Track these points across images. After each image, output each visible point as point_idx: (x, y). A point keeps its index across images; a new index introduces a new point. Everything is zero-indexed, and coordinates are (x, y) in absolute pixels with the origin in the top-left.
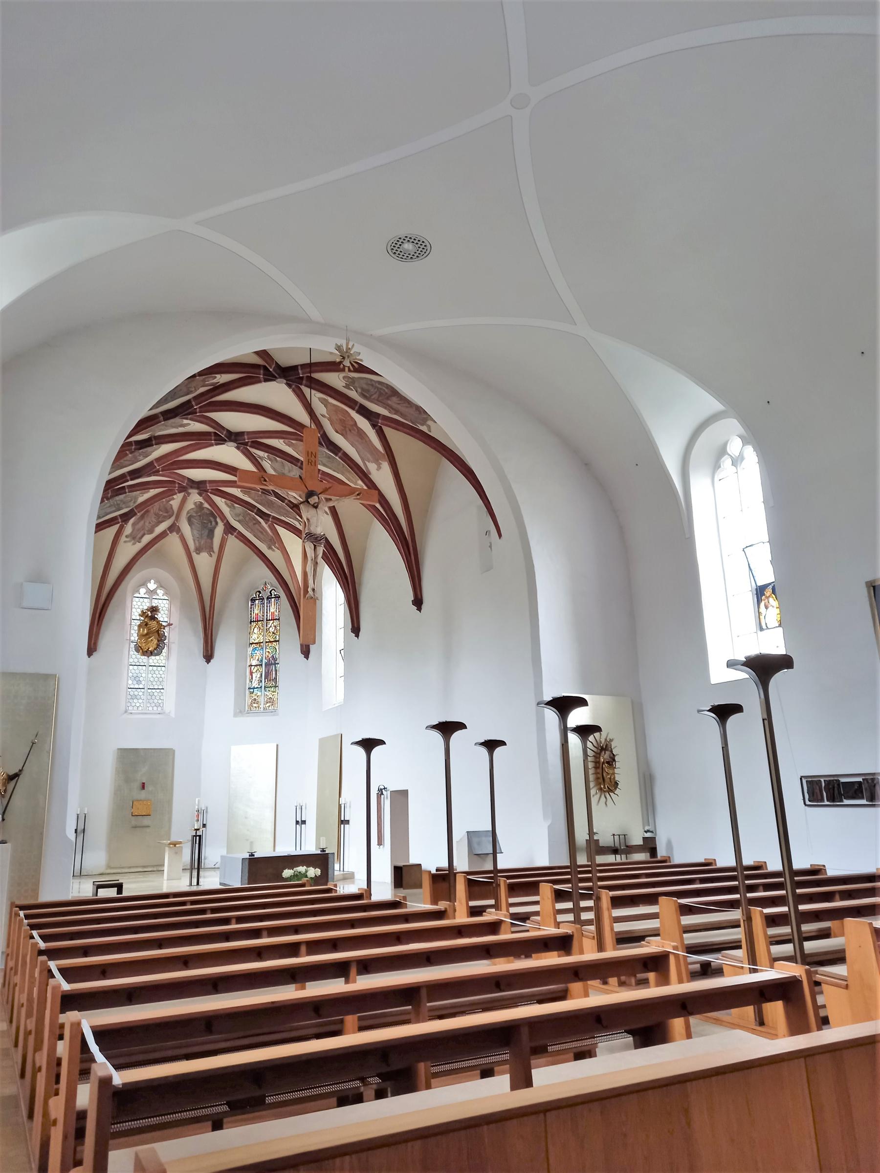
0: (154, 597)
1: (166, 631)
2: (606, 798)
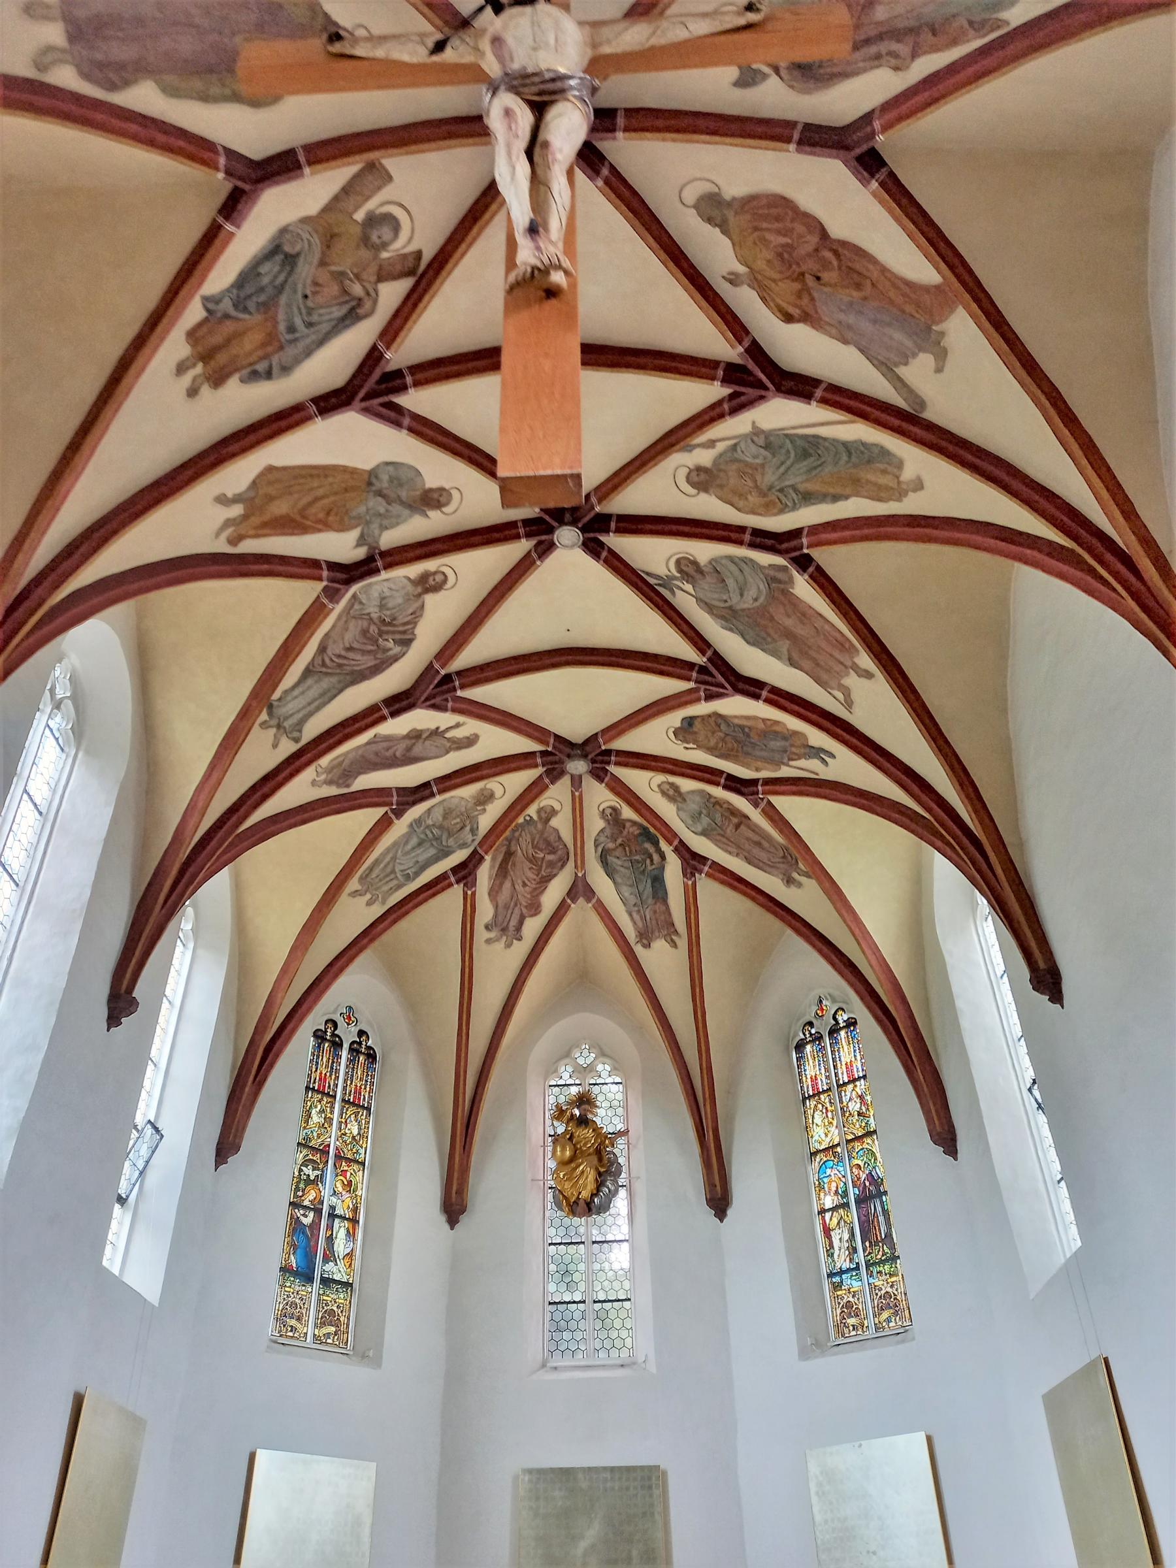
0: (592, 1081)
1: (620, 1149)
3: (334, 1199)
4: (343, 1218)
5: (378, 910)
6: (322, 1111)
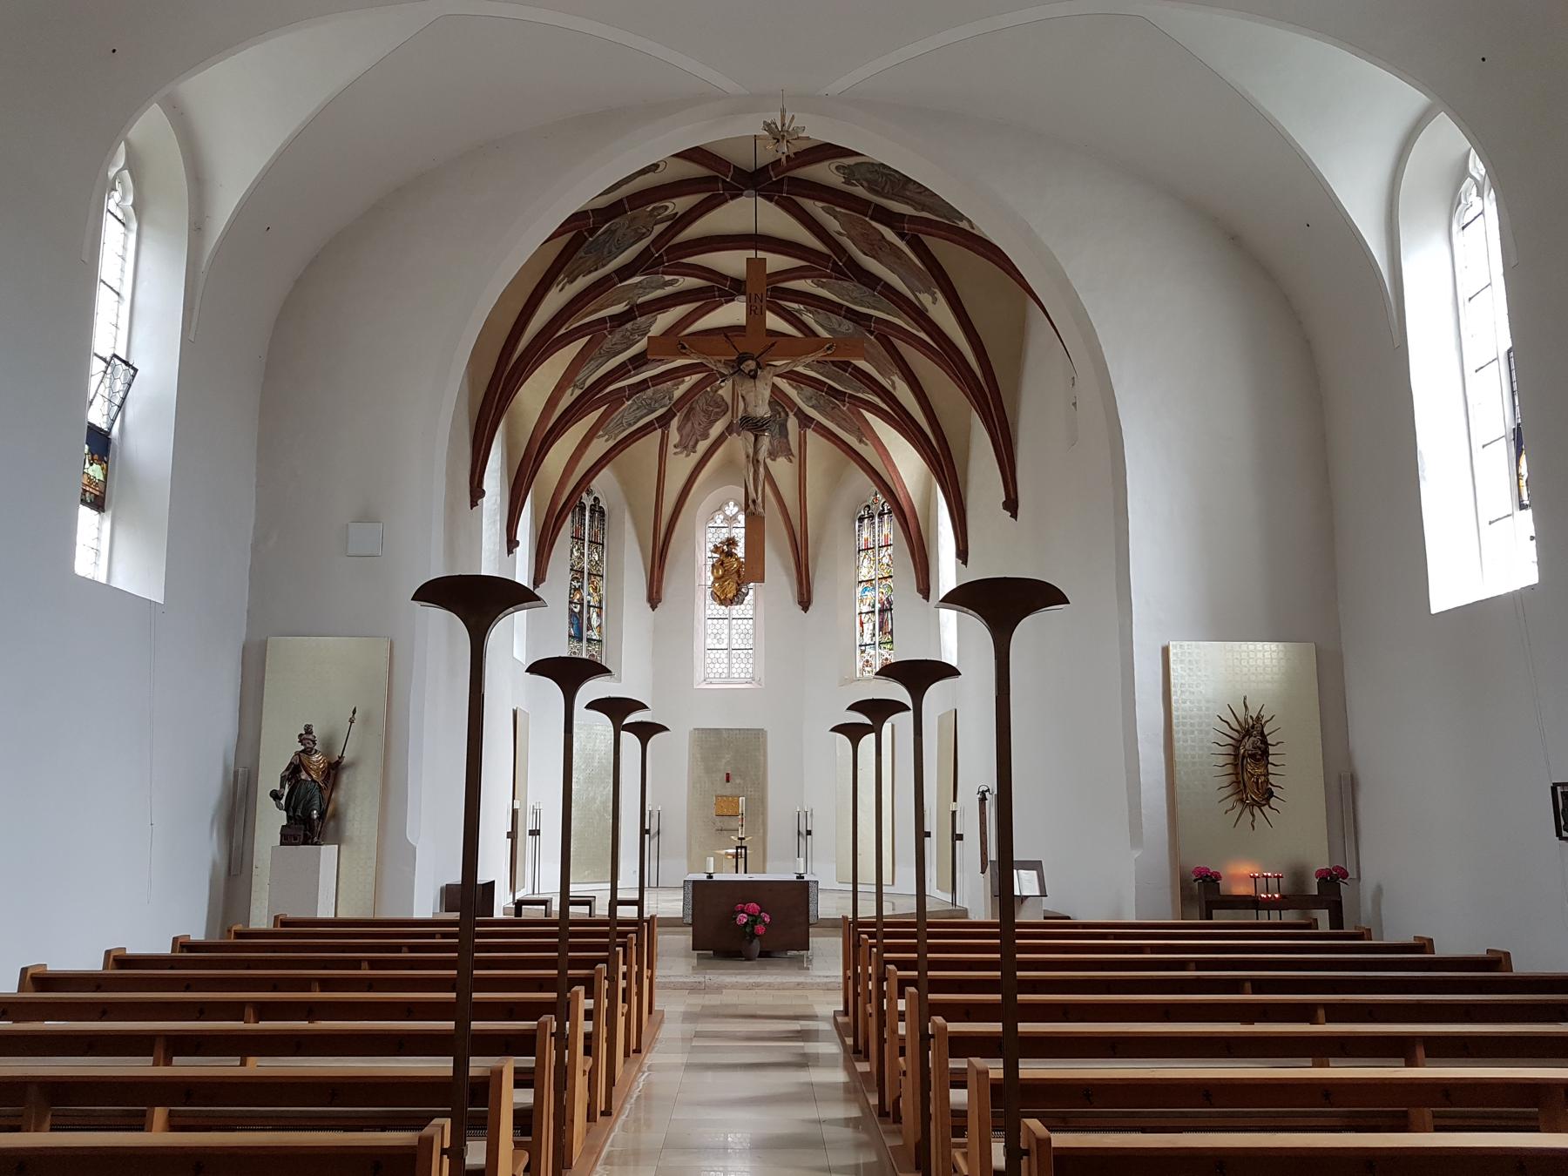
0: (735, 525)
2: (1253, 815)
3: (589, 597)
4: (595, 607)
5: (611, 443)
6: (579, 549)
